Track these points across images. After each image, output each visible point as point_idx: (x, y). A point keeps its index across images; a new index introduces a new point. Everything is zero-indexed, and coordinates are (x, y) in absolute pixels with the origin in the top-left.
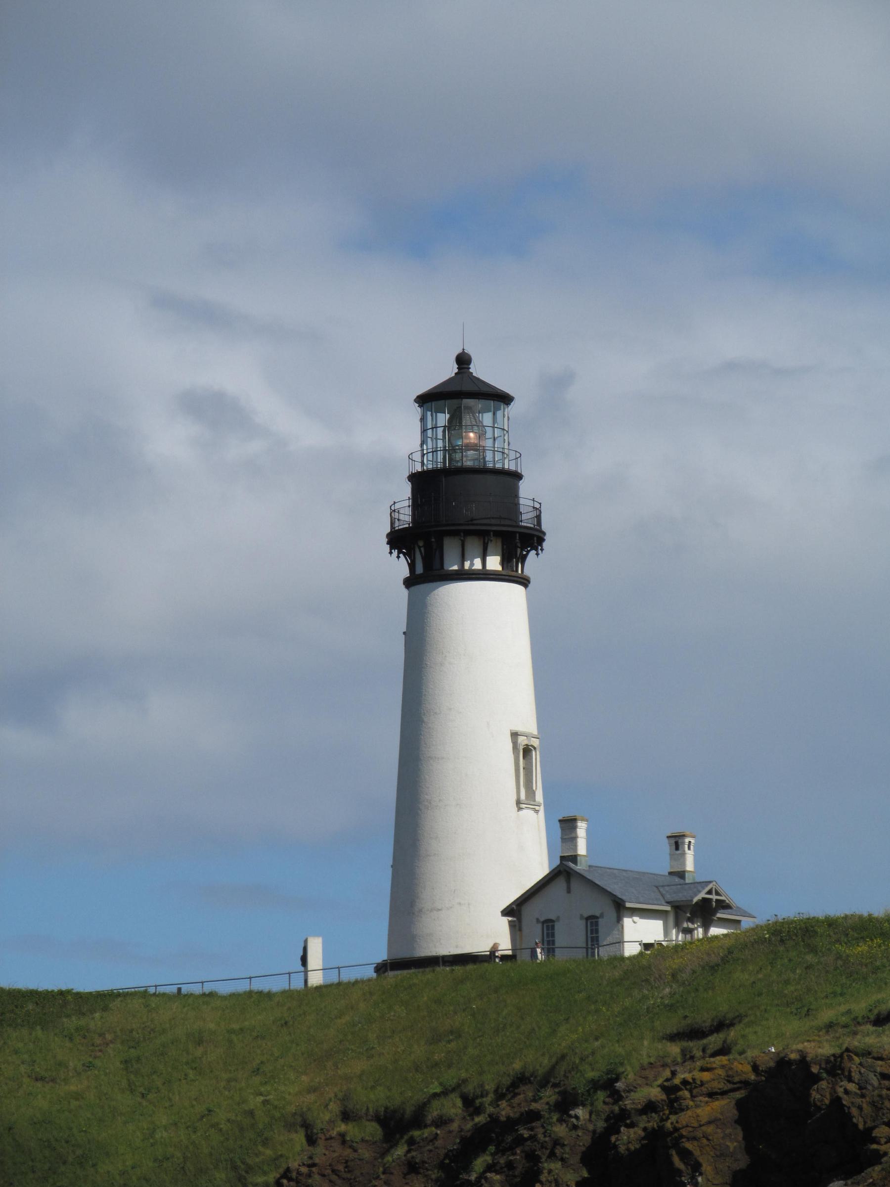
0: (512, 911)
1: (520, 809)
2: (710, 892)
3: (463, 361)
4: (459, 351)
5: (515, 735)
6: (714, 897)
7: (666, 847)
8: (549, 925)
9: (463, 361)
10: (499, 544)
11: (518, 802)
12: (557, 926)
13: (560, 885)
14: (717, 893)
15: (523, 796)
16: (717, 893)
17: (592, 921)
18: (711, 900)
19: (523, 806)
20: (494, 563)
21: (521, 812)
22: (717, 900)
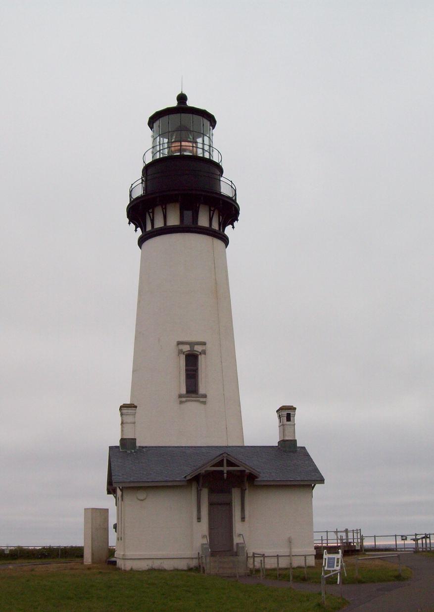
1: (181, 402)
2: (220, 464)
3: (182, 98)
4: (180, 93)
5: (179, 343)
6: (225, 469)
7: (274, 419)
9: (182, 98)
11: (180, 396)
14: (230, 464)
15: (183, 391)
18: (222, 472)
19: (184, 399)
20: (174, 220)
21: (183, 406)
22: (228, 472)
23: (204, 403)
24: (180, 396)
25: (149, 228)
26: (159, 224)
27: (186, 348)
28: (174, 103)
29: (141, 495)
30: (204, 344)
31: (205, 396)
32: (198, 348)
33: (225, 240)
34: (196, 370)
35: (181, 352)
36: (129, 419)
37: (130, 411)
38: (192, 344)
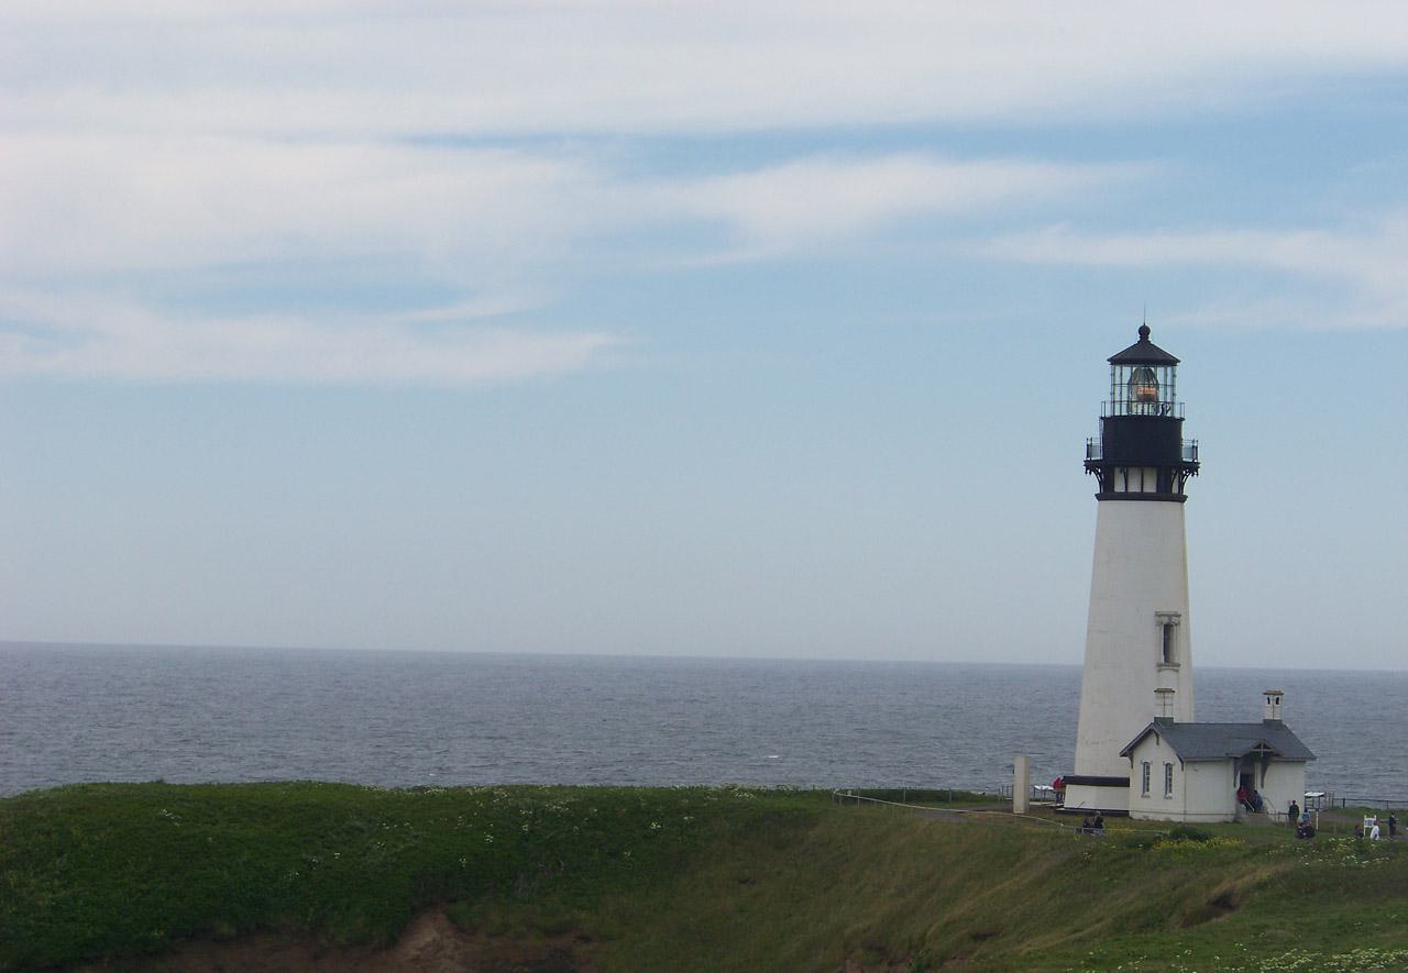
0: (1129, 752)
1: (1159, 671)
2: (1259, 747)
3: (1144, 331)
5: (1158, 615)
8: (1147, 766)
9: (1144, 331)
10: (1155, 473)
11: (1160, 665)
12: (1151, 767)
13: (1152, 740)
14: (1265, 747)
16: (1265, 747)
17: (1169, 767)
20: (1150, 488)
22: (1264, 753)
23: (1177, 671)
24: (1160, 665)
25: (1119, 487)
26: (1134, 488)
27: (1166, 620)
28: (1136, 338)
29: (1197, 767)
30: (1179, 616)
31: (1179, 665)
32: (1174, 619)
33: (1181, 499)
34: (1169, 639)
35: (1159, 624)
36: (1167, 701)
37: (1170, 695)
38: (1170, 616)
